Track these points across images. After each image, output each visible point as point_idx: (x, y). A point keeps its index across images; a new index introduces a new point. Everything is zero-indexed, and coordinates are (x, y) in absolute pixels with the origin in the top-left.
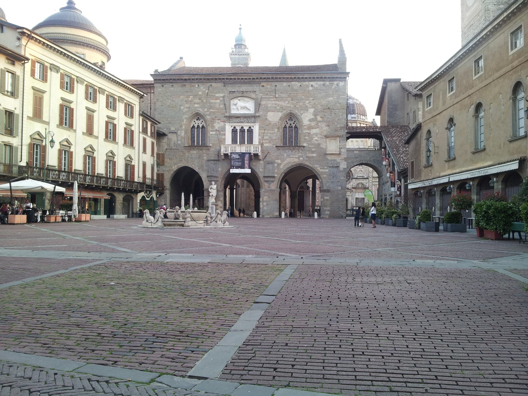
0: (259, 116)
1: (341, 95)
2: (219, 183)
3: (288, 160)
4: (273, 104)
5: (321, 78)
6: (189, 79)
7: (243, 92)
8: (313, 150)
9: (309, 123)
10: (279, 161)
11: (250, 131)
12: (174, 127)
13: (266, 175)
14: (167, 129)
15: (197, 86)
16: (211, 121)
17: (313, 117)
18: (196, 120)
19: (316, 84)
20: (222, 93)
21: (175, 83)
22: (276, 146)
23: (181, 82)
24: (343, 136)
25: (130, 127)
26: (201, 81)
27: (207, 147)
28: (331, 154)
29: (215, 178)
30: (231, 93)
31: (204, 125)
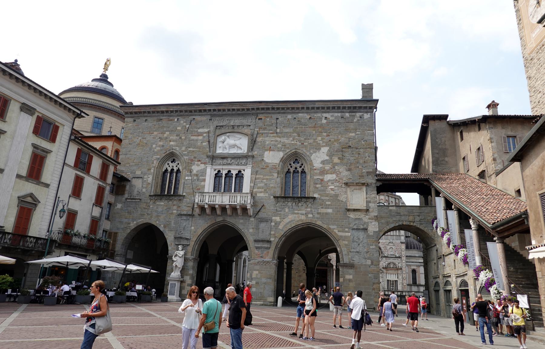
0: (253, 157)
1: (366, 130)
2: (190, 249)
3: (291, 217)
4: (272, 141)
5: (339, 108)
6: (167, 112)
7: (233, 127)
8: (328, 203)
9: (321, 165)
10: (278, 219)
11: (240, 176)
12: (140, 170)
13: (258, 238)
14: (131, 173)
15: (176, 120)
16: (188, 163)
17: (327, 158)
18: (170, 163)
19: (332, 116)
20: (207, 128)
21: (150, 116)
22: (274, 197)
23: (158, 116)
24: (371, 184)
25: (45, 153)
26: (182, 114)
27: (181, 197)
28: (355, 210)
29: (186, 241)
30: (219, 127)
31: (181, 169)
